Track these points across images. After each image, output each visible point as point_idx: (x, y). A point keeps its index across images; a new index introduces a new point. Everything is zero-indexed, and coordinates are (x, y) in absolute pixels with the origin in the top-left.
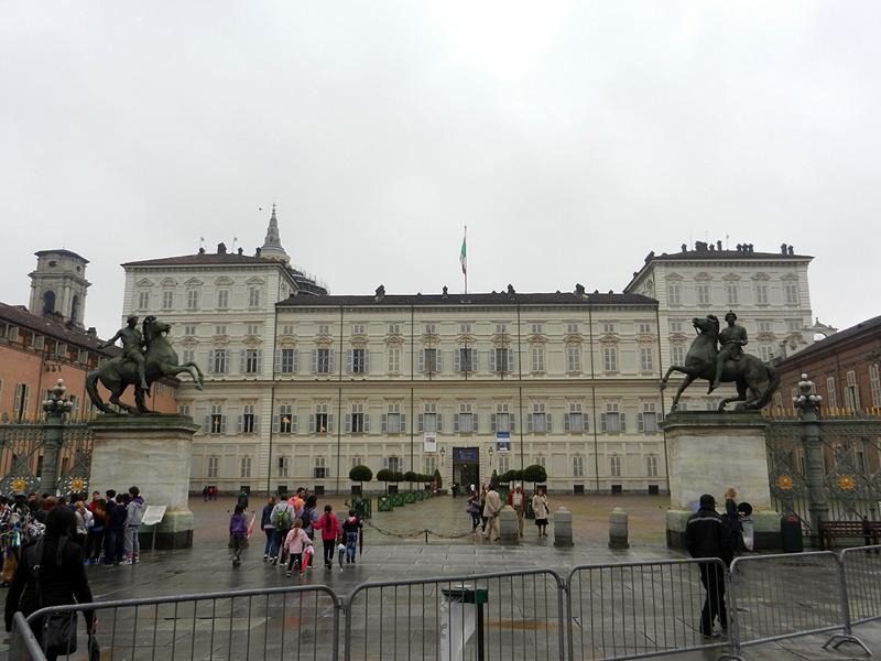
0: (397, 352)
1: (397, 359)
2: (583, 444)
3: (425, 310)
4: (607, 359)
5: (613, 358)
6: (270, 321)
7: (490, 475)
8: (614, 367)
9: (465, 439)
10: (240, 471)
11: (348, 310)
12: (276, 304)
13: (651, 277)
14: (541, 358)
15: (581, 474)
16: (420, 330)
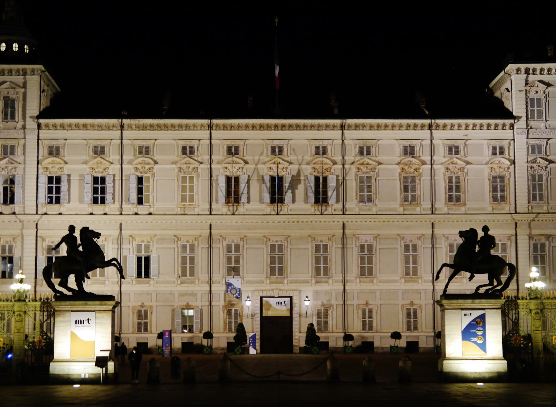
0: (191, 178)
1: (192, 189)
2: (418, 292)
3: (225, 127)
4: (450, 189)
5: (458, 188)
6: (32, 138)
7: (304, 329)
8: (458, 199)
9: (274, 286)
10: (31, 327)
11: (130, 127)
12: (38, 117)
13: (507, 85)
14: (369, 187)
15: (416, 328)
16: (220, 154)
